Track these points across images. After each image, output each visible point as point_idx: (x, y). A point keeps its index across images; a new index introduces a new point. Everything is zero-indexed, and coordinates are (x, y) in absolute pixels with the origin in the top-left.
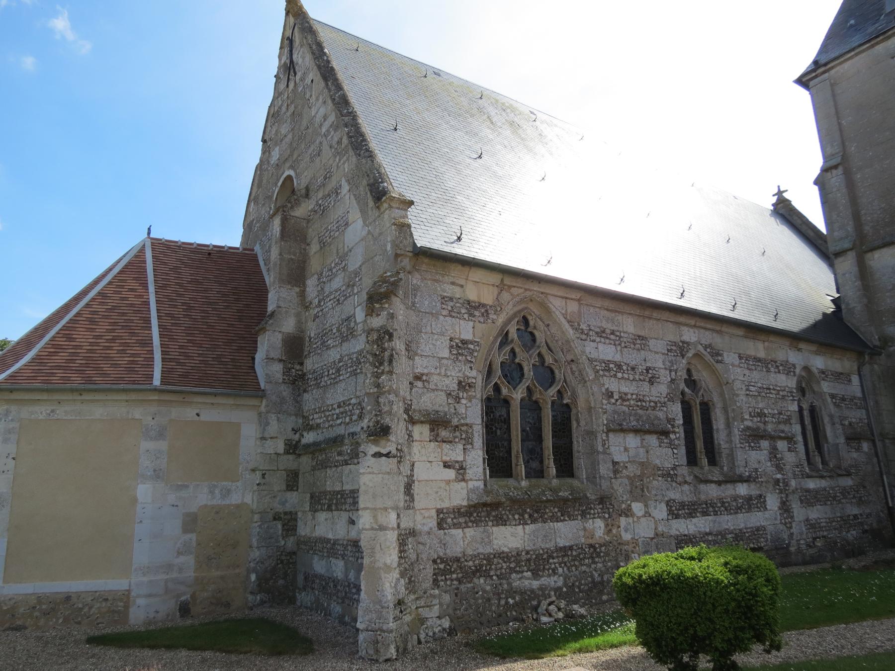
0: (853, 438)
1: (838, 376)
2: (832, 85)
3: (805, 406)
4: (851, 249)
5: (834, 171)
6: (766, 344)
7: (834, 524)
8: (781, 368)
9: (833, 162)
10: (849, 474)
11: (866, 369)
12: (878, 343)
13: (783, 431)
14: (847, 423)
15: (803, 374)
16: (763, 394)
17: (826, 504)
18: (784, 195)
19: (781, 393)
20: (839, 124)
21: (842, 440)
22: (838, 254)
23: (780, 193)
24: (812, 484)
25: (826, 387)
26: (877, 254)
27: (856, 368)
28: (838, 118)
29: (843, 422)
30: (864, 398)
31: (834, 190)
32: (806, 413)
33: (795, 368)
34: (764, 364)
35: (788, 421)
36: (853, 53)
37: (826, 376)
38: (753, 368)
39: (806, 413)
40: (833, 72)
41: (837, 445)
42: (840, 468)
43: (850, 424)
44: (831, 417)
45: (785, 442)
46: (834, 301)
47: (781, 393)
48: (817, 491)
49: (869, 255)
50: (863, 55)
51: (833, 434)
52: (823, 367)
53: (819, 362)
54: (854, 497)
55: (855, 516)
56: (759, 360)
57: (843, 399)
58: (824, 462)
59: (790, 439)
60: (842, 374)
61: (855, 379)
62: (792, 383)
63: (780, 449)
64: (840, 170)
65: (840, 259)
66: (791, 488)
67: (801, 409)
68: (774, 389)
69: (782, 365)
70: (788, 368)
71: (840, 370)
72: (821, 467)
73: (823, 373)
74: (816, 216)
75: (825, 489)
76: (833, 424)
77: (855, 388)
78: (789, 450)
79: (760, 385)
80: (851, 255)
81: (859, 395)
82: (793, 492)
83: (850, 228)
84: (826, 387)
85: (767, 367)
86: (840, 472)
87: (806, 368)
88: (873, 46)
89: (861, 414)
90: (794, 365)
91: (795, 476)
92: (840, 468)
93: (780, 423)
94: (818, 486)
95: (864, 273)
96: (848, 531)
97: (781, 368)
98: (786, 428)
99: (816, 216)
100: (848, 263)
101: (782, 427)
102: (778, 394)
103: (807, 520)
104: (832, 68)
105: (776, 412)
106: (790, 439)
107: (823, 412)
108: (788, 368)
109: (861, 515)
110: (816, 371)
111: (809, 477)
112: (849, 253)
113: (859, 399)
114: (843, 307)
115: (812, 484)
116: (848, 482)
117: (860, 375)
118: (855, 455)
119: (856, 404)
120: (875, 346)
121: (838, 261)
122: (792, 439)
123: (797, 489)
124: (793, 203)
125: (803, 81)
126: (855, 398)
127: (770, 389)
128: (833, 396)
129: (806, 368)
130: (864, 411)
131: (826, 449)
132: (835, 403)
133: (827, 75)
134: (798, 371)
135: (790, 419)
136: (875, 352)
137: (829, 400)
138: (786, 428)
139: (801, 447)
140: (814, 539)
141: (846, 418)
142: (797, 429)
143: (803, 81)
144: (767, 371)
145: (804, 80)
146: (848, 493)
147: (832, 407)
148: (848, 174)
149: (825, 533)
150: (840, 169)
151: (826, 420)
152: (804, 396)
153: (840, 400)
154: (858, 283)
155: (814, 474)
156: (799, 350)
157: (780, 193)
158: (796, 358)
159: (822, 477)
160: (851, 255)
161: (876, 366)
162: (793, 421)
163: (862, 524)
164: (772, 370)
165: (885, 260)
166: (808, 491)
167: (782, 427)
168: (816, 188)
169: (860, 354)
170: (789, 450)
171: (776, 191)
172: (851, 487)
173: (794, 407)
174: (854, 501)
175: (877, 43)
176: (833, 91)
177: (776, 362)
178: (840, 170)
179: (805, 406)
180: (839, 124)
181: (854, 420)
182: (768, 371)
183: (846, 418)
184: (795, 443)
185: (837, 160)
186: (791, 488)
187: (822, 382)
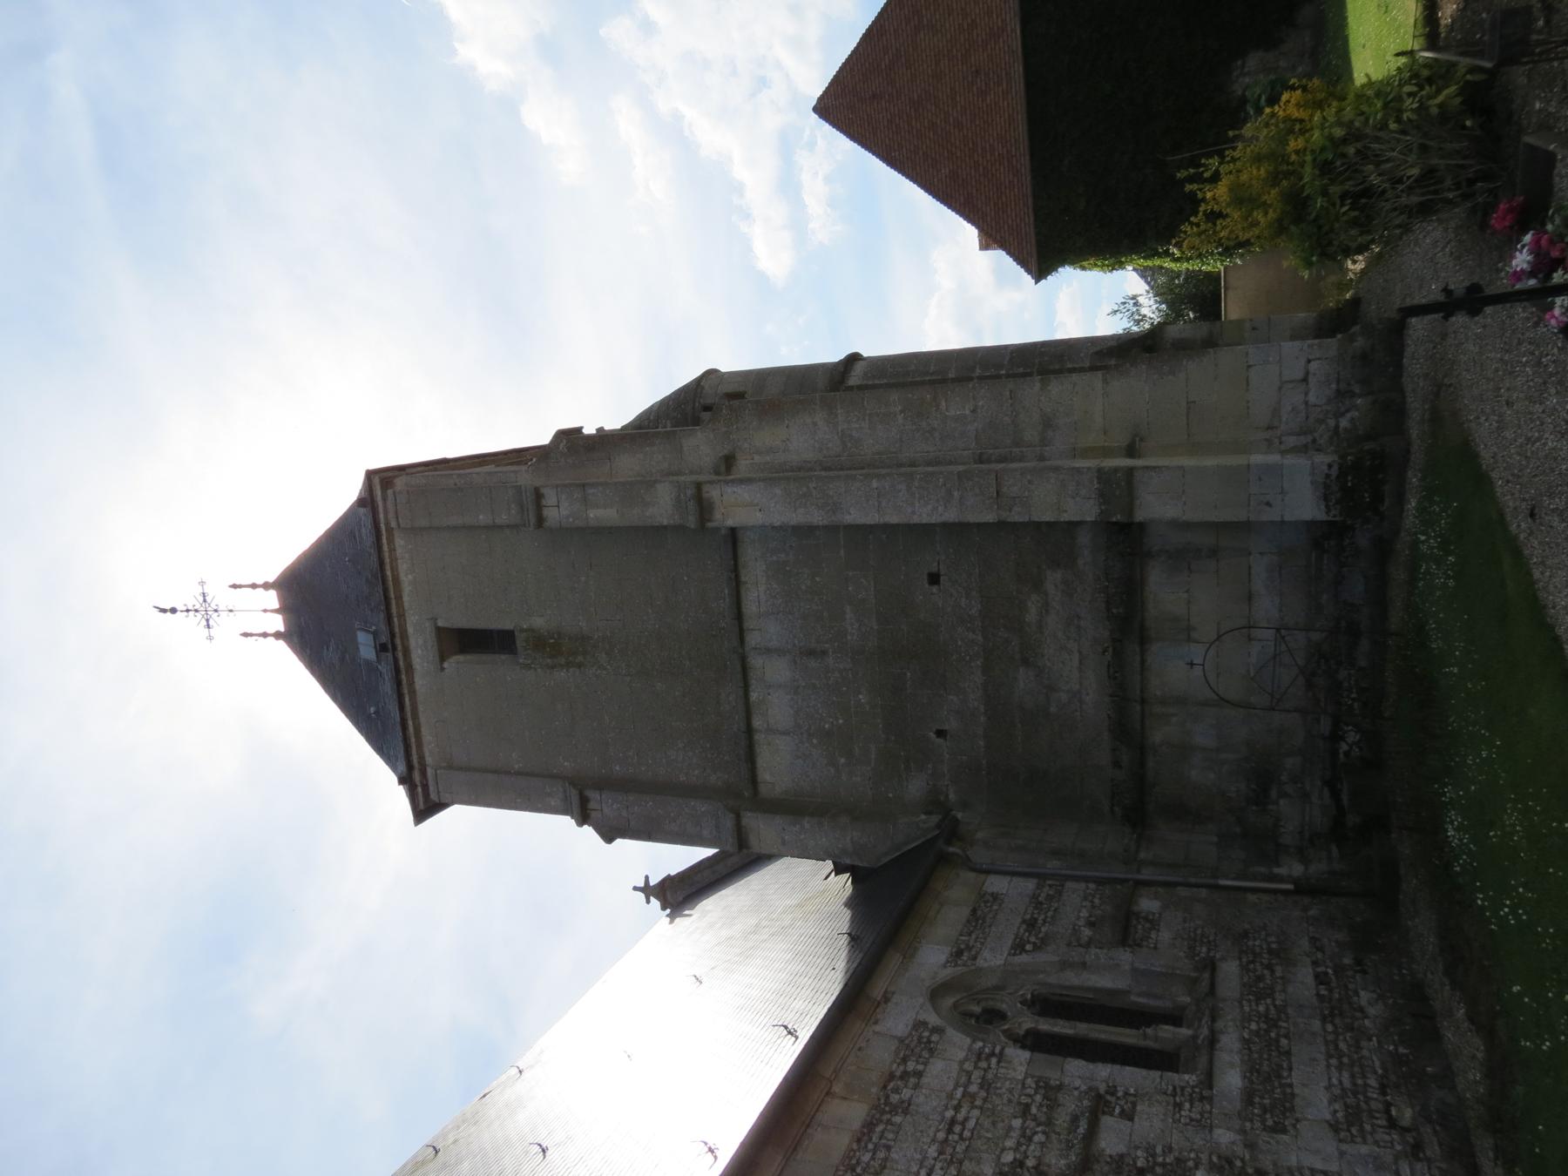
0: (1125, 928)
1: (977, 919)
2: (450, 767)
3: (1027, 1022)
4: (738, 817)
5: (592, 805)
6: (837, 1088)
7: (1342, 1046)
8: (911, 1066)
9: (575, 800)
10: (1211, 966)
11: (980, 856)
12: (935, 819)
13: (1075, 1119)
14: (1087, 932)
15: (949, 1001)
16: (960, 1148)
17: (1288, 1053)
18: (652, 882)
19: (973, 1088)
20: (519, 773)
21: (1125, 956)
22: (742, 841)
23: (647, 890)
24: (1231, 1080)
25: (993, 957)
26: (764, 775)
27: (972, 875)
28: (508, 773)
29: (1084, 940)
30: (1041, 877)
31: (624, 813)
32: (1045, 1026)
33: (925, 1024)
34: (887, 1110)
35: (1052, 1093)
36: (410, 723)
37: (969, 948)
38: (881, 1154)
39: (1045, 1026)
40: (429, 760)
41: (1134, 970)
42: (1195, 981)
43: (1091, 924)
44: (1064, 965)
45: (1107, 1121)
46: (839, 870)
47: (973, 1088)
48: (1251, 1069)
49: (763, 789)
50: (421, 708)
51: (1108, 973)
52: (947, 950)
53: (931, 959)
54: (1270, 967)
55: (1320, 979)
56: (869, 1125)
57: (1031, 924)
58: (1175, 1019)
59: (1099, 1104)
60: (974, 911)
61: (996, 884)
62: (958, 1044)
63: (1122, 1149)
64: (593, 795)
65: (753, 841)
66: (1239, 1150)
67: (1036, 1042)
68: (957, 1108)
69: (905, 1060)
70: (921, 1044)
71: (965, 912)
72: (1185, 1032)
73: (959, 953)
74: (679, 857)
75: (1246, 1043)
76: (1084, 965)
77: (1013, 890)
78: (1128, 1116)
79: (932, 1151)
80: (751, 820)
81: (1030, 885)
82: (1251, 1146)
83: (702, 807)
84: (993, 957)
85: (894, 1110)
86: (1204, 985)
87: (935, 994)
88: (413, 692)
89: (1074, 894)
90: (919, 1025)
91: (1203, 1124)
92: (1195, 981)
93: (1049, 1122)
94: (1237, 1059)
95: (792, 807)
96: (1362, 1010)
97: (911, 1066)
98: (1069, 1105)
99: (679, 857)
100: (762, 829)
101: (1062, 1119)
102: (973, 1097)
103: (1335, 1127)
104: (421, 758)
105: (1017, 1123)
106: (1099, 1104)
107: (1052, 980)
108: (921, 1044)
109: (1315, 963)
110: (948, 972)
111: (1209, 1080)
112: (745, 821)
113: (1039, 887)
114: (848, 861)
115: (1231, 1080)
116: (1230, 970)
117: (988, 872)
118: (1165, 936)
119: (1050, 898)
120: (938, 826)
121: (756, 846)
122: (1099, 1097)
123: (1243, 1131)
124: (673, 873)
125: (424, 808)
126: (1035, 897)
127: (953, 1122)
128: (1019, 947)
129: (935, 994)
130: (1069, 885)
131: (1141, 1000)
132: (1036, 948)
133: (430, 772)
134: (933, 1019)
135: (1047, 1087)
136: (951, 831)
137: (1024, 958)
138: (1069, 1105)
139: (1129, 1077)
140: (1392, 1124)
141: (1076, 931)
142: (1076, 1071)
143: (424, 808)
144: (906, 1112)
145: (422, 806)
146: (1260, 978)
147: (1042, 957)
148: (606, 784)
149: (1373, 1082)
150: (590, 793)
151: (1072, 978)
152: (1002, 1016)
153: (1031, 935)
154: (807, 823)
155: (1203, 1061)
156: (886, 999)
157: (647, 890)
158: (897, 1020)
159: (1213, 1041)
160: (751, 820)
161: (980, 835)
162: (1054, 1077)
163: (1339, 970)
164: (906, 1093)
165: (779, 765)
166: (1249, 1097)
167: (1062, 1119)
168: (619, 842)
169: (944, 860)
170: (1128, 1116)
171: (642, 896)
172: (1245, 968)
173: (1019, 1057)
174: (1279, 971)
175: (411, 683)
176: (460, 769)
177: (892, 1076)
178: (593, 795)
179: (1027, 1022)
180: (519, 773)
181: (1084, 913)
182: (905, 1108)
183: (1076, 931)
184: (1112, 1091)
185: (574, 793)
186: (1239, 1150)
187: (980, 962)
